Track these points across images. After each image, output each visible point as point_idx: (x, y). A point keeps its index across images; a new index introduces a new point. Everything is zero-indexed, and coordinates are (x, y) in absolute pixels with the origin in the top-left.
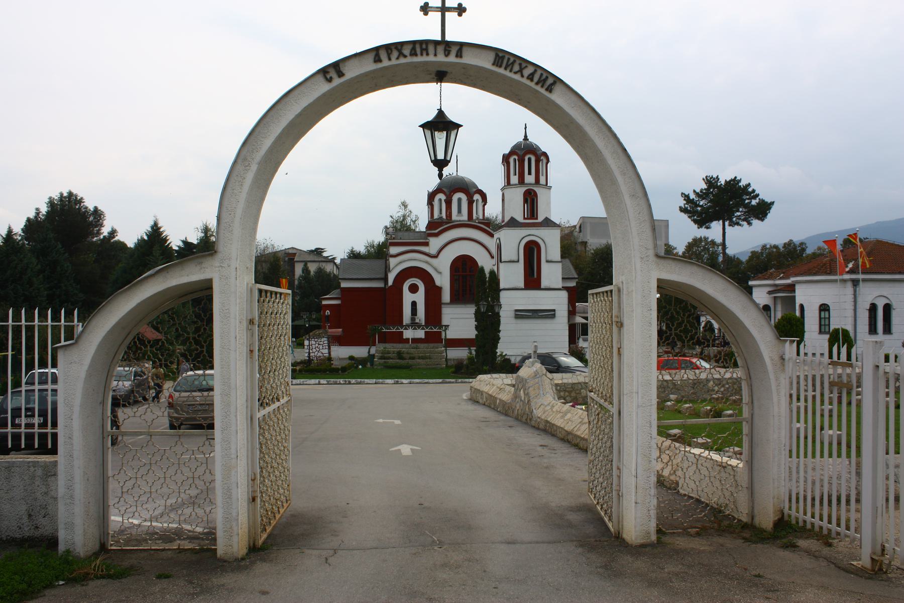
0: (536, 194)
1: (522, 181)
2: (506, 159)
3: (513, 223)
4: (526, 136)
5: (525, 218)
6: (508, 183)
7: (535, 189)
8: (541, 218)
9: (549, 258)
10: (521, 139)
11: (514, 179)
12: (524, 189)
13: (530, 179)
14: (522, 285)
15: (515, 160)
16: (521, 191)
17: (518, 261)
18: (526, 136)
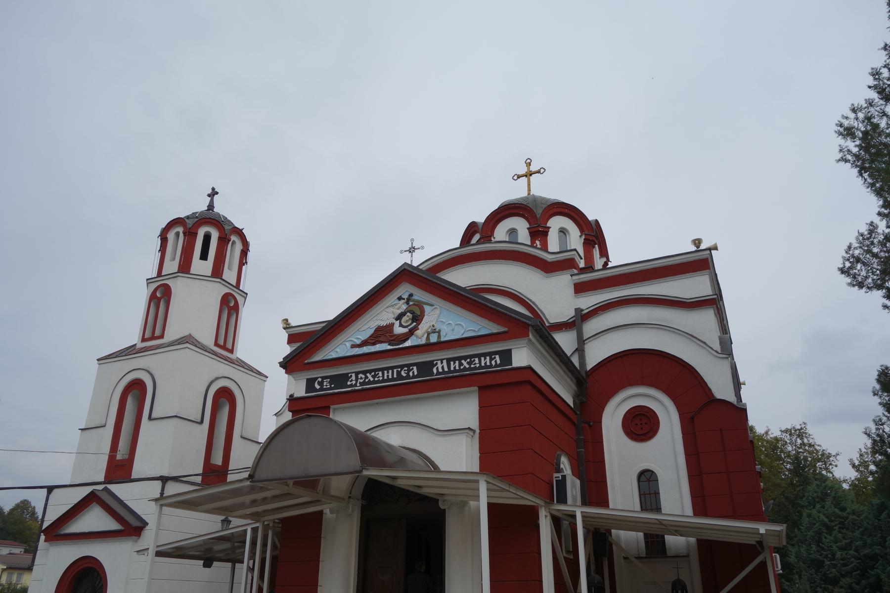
1: (217, 273)
4: (211, 207)
5: (216, 344)
6: (185, 267)
10: (201, 206)
13: (229, 275)
16: (217, 291)
17: (202, 422)
18: (211, 207)
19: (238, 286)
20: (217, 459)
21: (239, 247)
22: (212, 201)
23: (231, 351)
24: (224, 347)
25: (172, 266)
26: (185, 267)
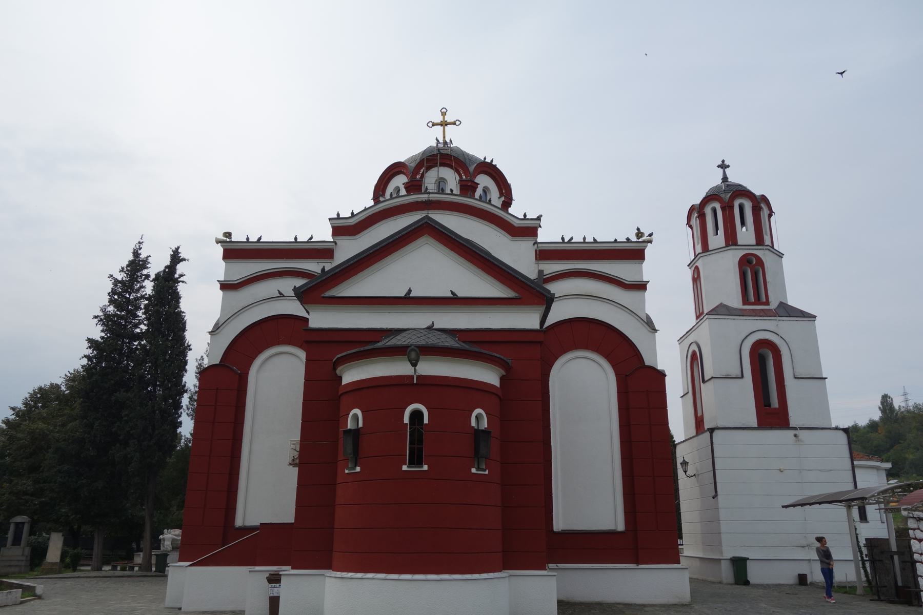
0: (760, 262)
1: (731, 239)
2: (697, 212)
3: (721, 310)
4: (725, 179)
6: (705, 248)
7: (759, 253)
8: (774, 305)
9: (801, 372)
10: (717, 181)
11: (717, 240)
12: (741, 253)
13: (746, 235)
14: (754, 422)
15: (714, 211)
16: (732, 257)
17: (742, 376)
18: (725, 179)
19: (760, 241)
20: (775, 403)
21: (748, 206)
22: (724, 173)
23: (767, 303)
24: (758, 301)
25: (699, 249)
26: (705, 248)
